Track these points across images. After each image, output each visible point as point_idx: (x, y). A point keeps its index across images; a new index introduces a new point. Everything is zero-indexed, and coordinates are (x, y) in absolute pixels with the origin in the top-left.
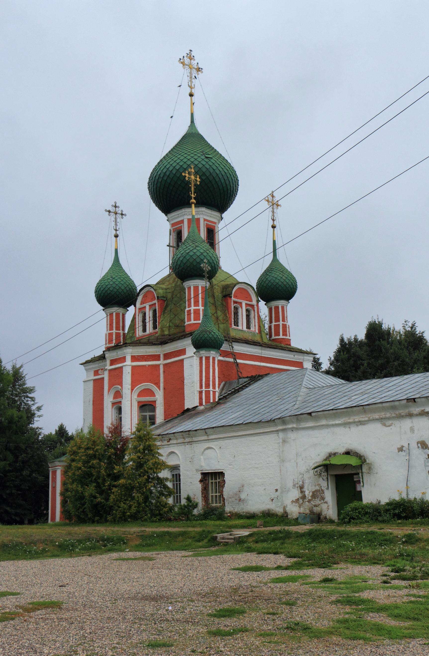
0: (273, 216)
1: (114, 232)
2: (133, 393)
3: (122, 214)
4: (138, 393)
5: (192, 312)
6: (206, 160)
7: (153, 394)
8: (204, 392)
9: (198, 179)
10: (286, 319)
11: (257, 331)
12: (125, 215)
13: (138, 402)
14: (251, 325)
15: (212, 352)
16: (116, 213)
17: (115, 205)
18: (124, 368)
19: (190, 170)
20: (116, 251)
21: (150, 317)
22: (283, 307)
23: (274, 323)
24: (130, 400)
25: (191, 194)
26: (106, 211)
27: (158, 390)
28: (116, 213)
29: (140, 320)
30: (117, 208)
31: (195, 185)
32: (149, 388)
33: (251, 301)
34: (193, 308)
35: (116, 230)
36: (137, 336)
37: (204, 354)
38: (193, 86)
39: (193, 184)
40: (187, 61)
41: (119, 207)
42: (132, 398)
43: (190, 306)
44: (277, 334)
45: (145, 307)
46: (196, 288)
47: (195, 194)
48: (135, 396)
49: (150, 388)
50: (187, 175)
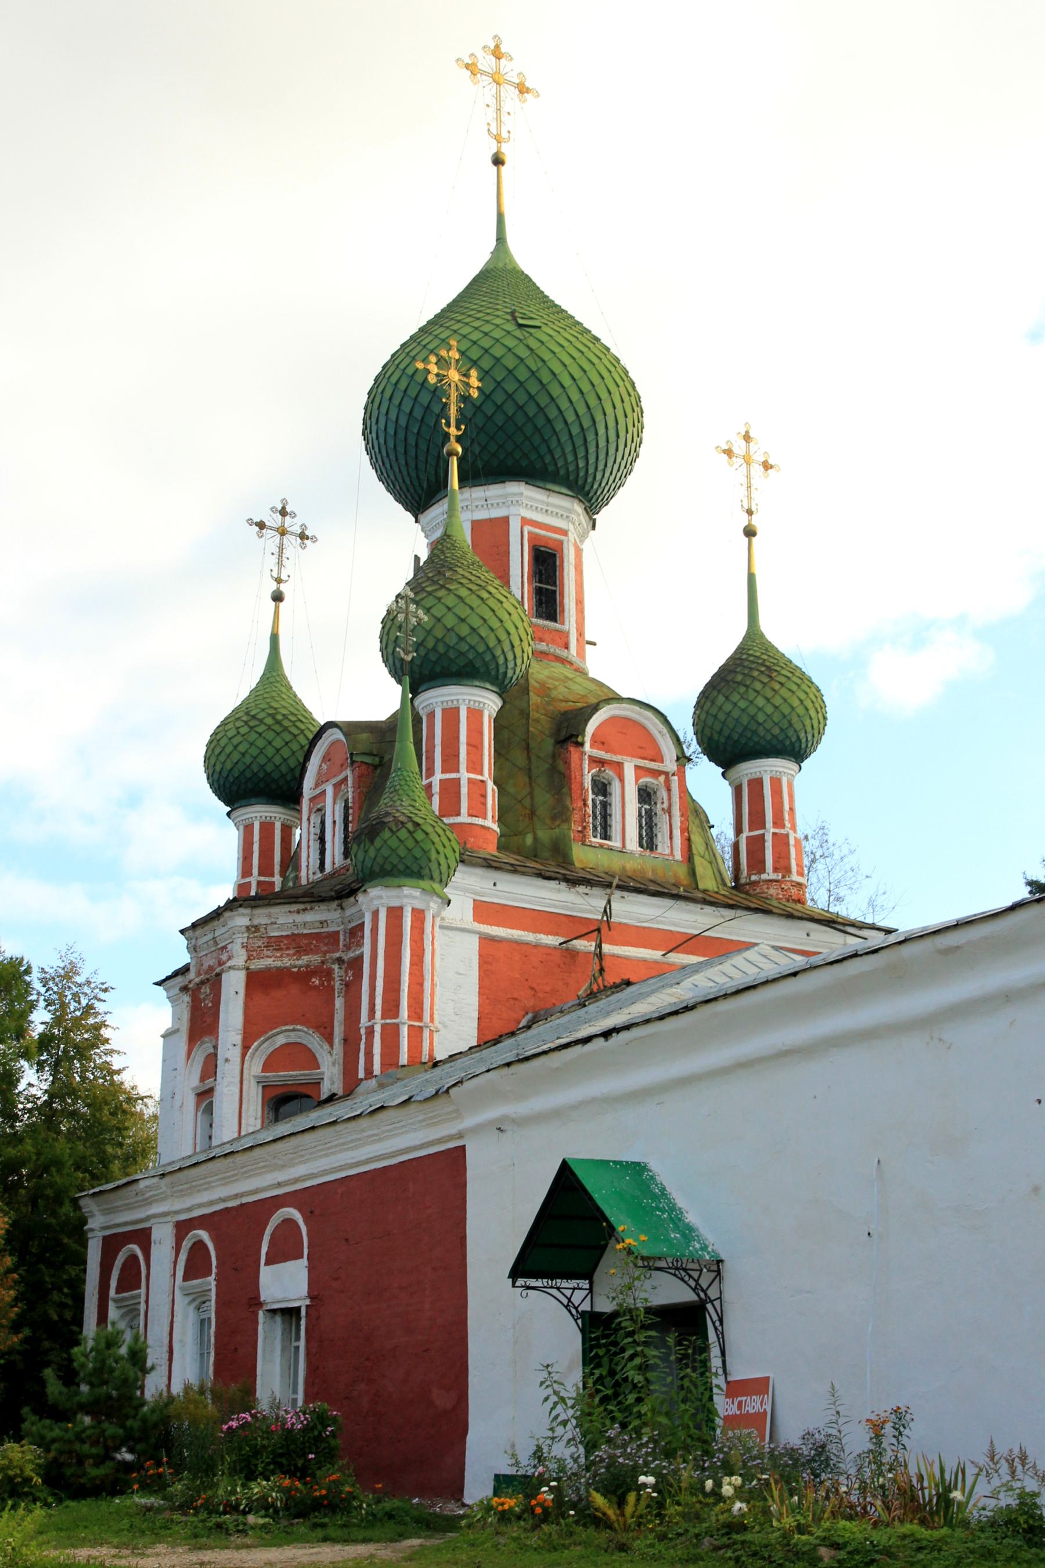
0: (749, 498)
1: (274, 586)
2: (247, 1058)
3: (303, 536)
4: (264, 1058)
5: (436, 789)
6: (518, 333)
7: (313, 1062)
8: (378, 1029)
9: (474, 382)
10: (786, 816)
11: (678, 856)
12: (314, 539)
13: (263, 1087)
14: (659, 835)
15: (406, 891)
16: (283, 532)
17: (284, 508)
18: (224, 976)
19: (443, 353)
20: (274, 639)
21: (334, 822)
22: (776, 783)
23: (746, 833)
24: (238, 1079)
25: (448, 425)
26: (250, 522)
27: (326, 1047)
28: (283, 532)
29: (312, 837)
30: (287, 518)
31: (465, 398)
32: (299, 1040)
33: (658, 757)
34: (438, 776)
35: (279, 581)
36: (304, 882)
37: (381, 897)
38: (505, 135)
39: (454, 395)
40: (487, 62)
41: (293, 515)
42: (245, 1071)
43: (430, 772)
44: (757, 863)
45: (324, 792)
46: (451, 715)
47: (463, 427)
48: (255, 1067)
49: (304, 1042)
50: (434, 369)
